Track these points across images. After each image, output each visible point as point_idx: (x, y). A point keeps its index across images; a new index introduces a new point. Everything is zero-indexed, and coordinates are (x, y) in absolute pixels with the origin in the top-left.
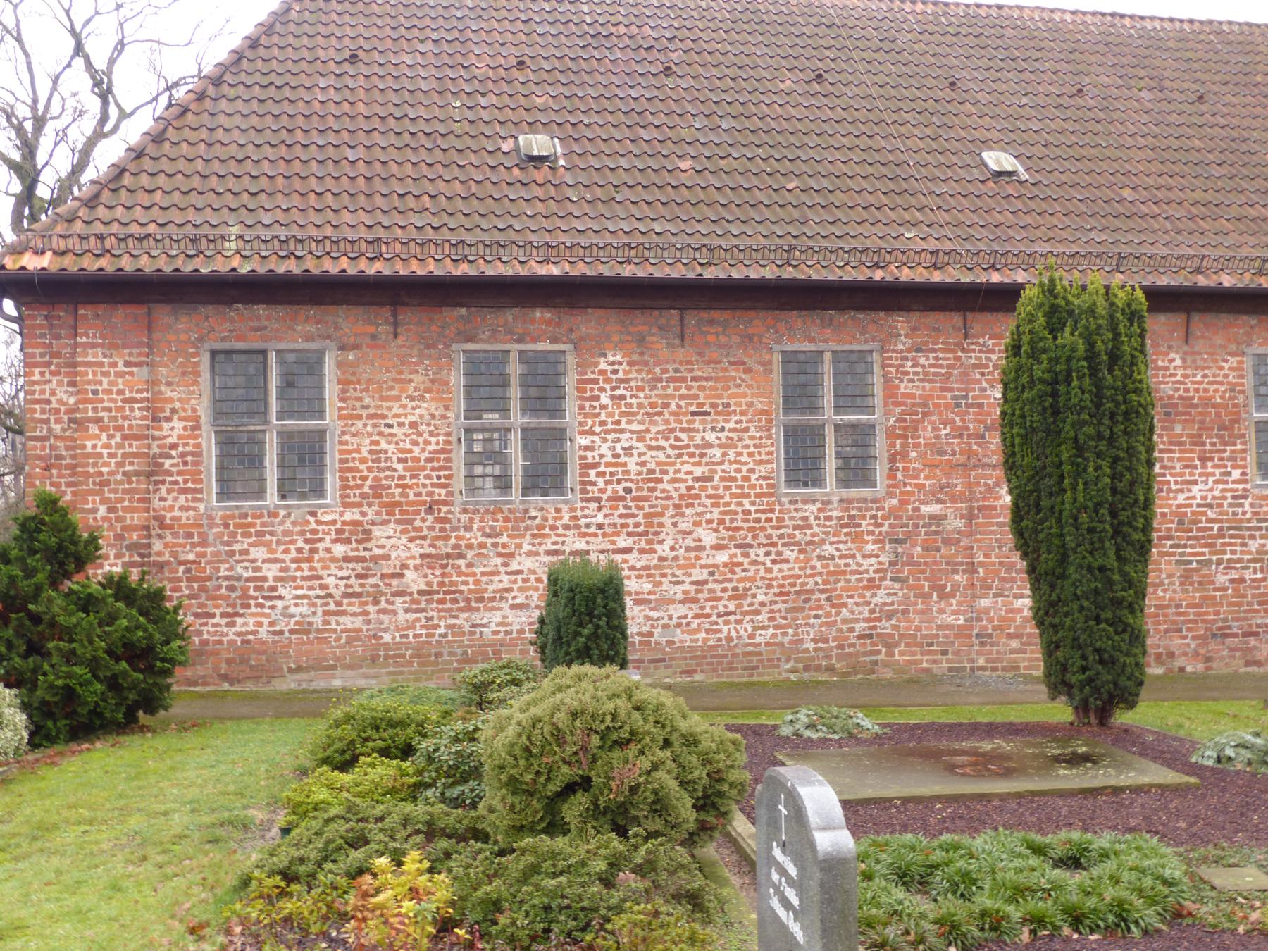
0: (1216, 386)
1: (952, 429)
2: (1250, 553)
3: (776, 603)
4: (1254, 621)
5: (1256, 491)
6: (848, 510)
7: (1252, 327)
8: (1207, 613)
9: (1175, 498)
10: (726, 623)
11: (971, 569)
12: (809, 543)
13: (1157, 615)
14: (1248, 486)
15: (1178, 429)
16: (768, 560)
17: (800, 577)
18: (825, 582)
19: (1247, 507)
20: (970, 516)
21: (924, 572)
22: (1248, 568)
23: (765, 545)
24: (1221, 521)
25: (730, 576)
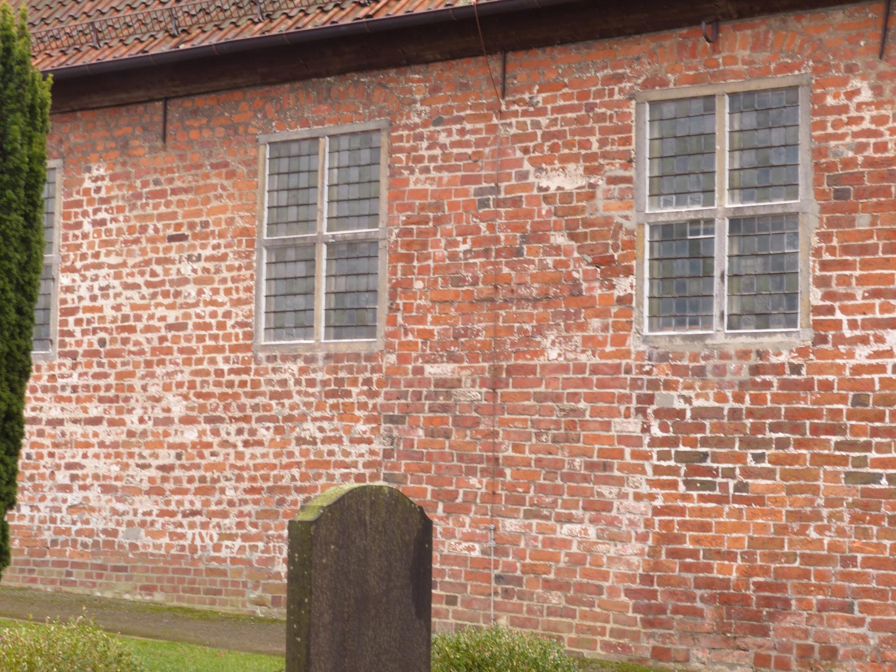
1: (474, 243)
3: (246, 502)
6: (335, 370)
9: (851, 355)
10: (192, 526)
11: (494, 469)
12: (289, 418)
13: (806, 575)
15: (863, 222)
16: (238, 440)
17: (273, 467)
18: (304, 477)
20: (494, 384)
21: (427, 470)
23: (237, 420)
25: (197, 460)
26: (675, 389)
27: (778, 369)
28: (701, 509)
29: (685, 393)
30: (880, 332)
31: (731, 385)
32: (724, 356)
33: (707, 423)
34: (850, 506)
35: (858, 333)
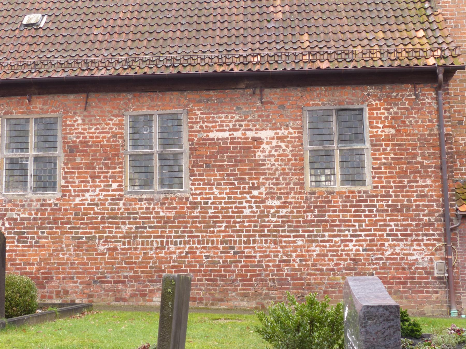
0: (104, 135)
2: (121, 233)
4: (122, 274)
5: (128, 196)
7: (129, 100)
8: (92, 268)
9: (74, 200)
13: (59, 268)
14: (123, 193)
15: (78, 160)
19: (121, 205)
22: (120, 242)
24: (104, 214)
26: (14, 211)
27: (50, 205)
28: (23, 250)
29: (18, 212)
30: (83, 193)
31: (34, 210)
32: (31, 201)
33: (25, 222)
34: (73, 247)
35: (76, 193)
